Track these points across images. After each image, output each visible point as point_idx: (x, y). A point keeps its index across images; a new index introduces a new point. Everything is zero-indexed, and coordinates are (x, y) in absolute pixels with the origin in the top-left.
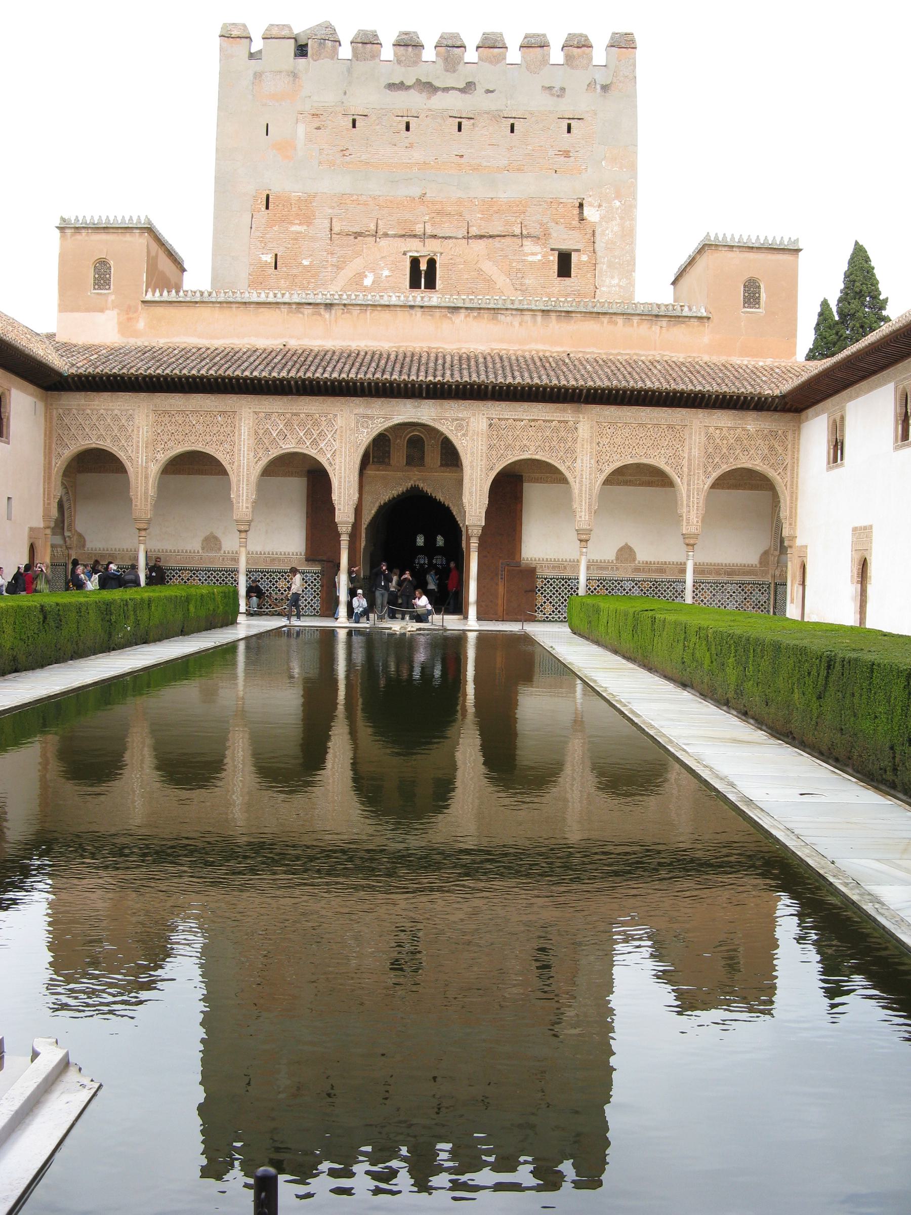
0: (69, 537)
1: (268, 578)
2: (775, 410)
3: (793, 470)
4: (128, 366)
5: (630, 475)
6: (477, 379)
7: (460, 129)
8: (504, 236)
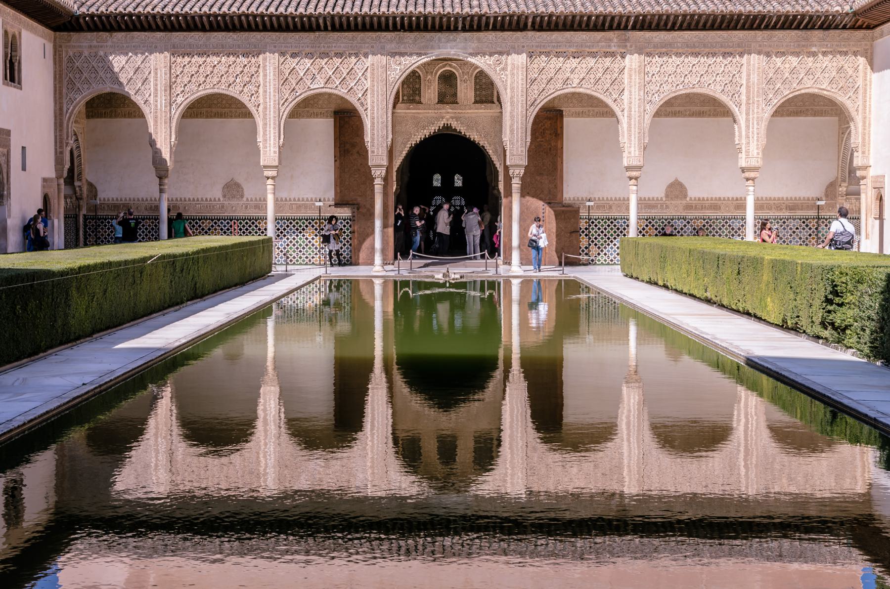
0: (79, 187)
1: (294, 226)
5: (679, 105)
6: (516, 10)
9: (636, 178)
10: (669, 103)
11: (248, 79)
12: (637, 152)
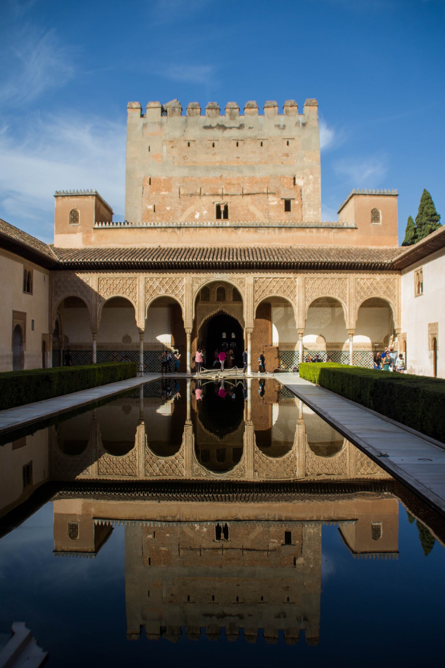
0: (61, 337)
1: (153, 355)
2: (389, 269)
3: (398, 297)
4: (87, 258)
6: (248, 260)
7: (237, 145)
8: (260, 193)
9: (302, 334)
10: (317, 301)
11: (132, 290)
12: (302, 322)
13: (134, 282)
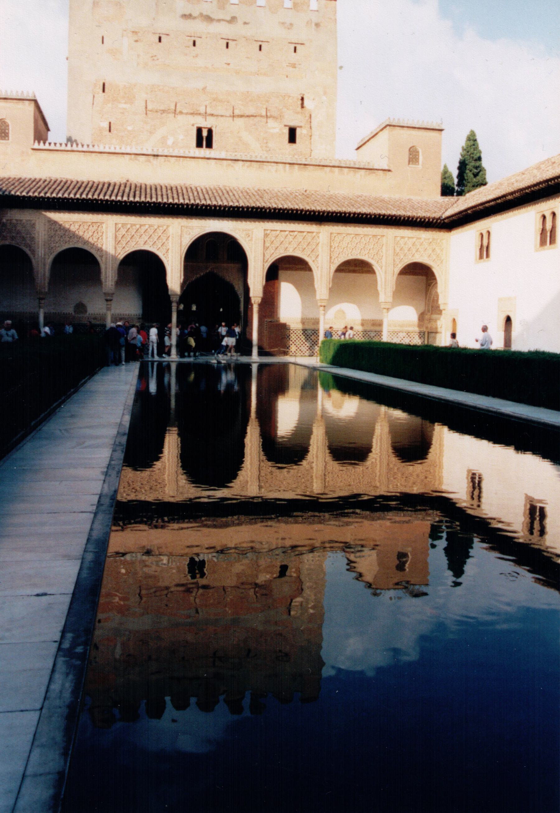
4: (33, 190)
7: (227, 47)
8: (256, 116)
9: (324, 306)
13: (99, 229)
